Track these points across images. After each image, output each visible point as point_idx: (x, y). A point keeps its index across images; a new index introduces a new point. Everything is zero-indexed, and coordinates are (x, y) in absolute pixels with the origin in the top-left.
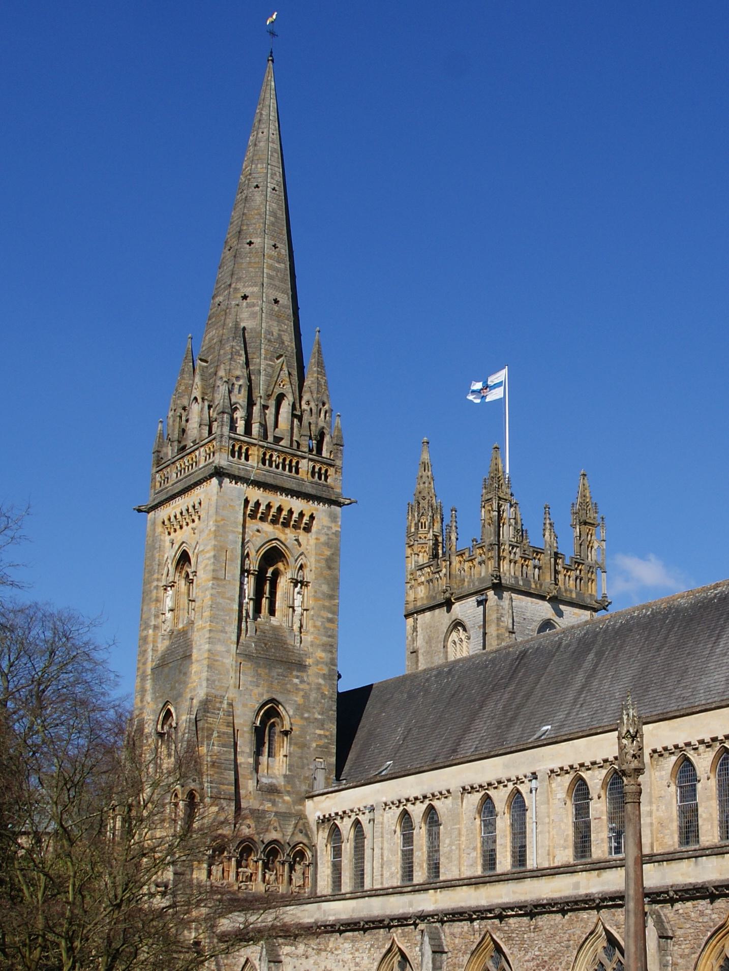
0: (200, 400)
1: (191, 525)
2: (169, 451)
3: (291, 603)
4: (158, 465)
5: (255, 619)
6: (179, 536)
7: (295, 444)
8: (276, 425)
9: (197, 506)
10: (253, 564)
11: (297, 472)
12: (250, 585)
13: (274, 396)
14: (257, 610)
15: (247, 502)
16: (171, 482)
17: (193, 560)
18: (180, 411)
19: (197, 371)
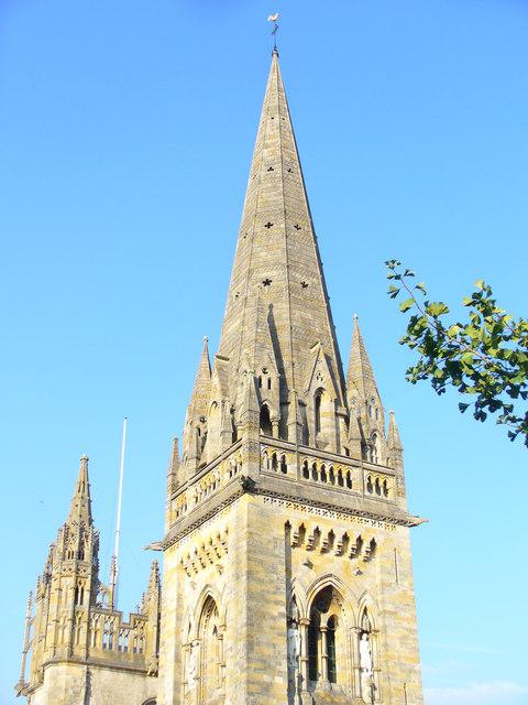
0: (220, 404)
1: (216, 561)
2: (186, 472)
3: (357, 662)
4: (173, 492)
5: (311, 687)
6: (203, 577)
7: (343, 453)
8: (318, 429)
9: (223, 535)
10: (303, 608)
11: (350, 485)
12: (300, 634)
13: (313, 391)
14: (313, 675)
15: (288, 526)
16: (190, 509)
17: (221, 609)
18: (197, 423)
19: (215, 372)
